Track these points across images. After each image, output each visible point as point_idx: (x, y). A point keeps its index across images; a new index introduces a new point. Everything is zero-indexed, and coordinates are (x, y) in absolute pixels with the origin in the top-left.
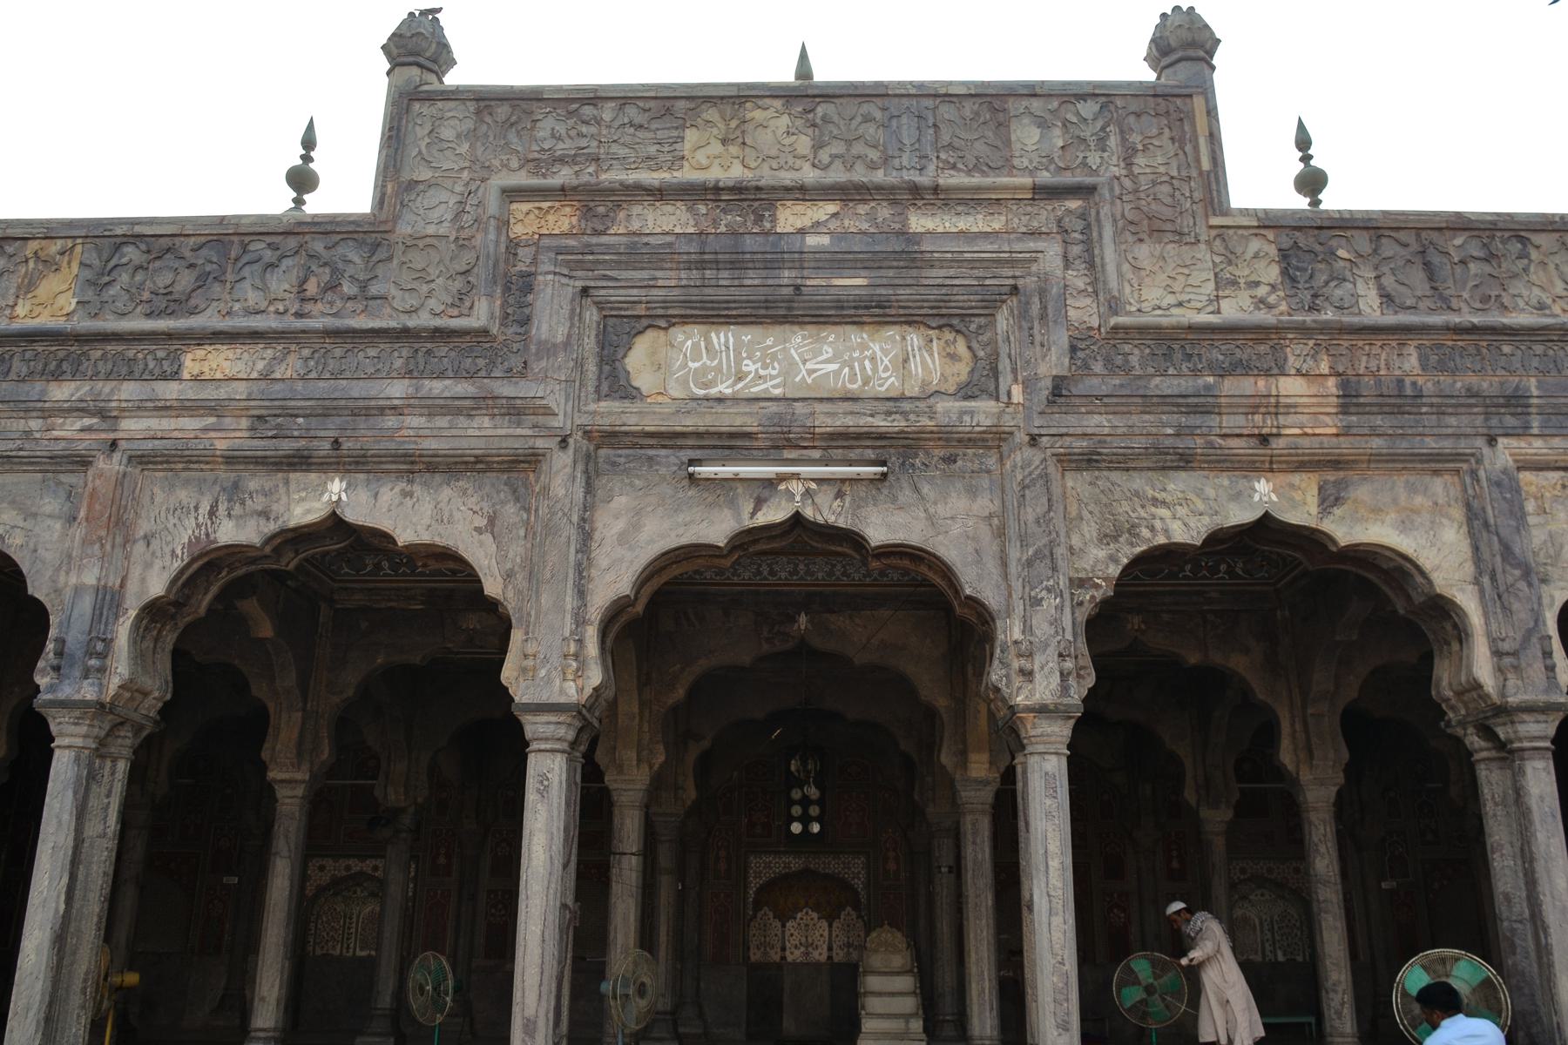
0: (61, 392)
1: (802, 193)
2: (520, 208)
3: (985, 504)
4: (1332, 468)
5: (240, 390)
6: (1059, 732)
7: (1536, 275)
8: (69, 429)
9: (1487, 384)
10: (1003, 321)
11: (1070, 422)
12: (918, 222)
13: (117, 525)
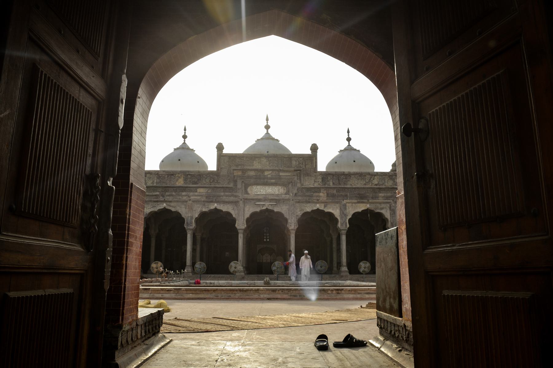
0: (184, 194)
3: (287, 207)
6: (294, 232)
7: (351, 181)
8: (185, 198)
12: (281, 174)
13: (191, 209)
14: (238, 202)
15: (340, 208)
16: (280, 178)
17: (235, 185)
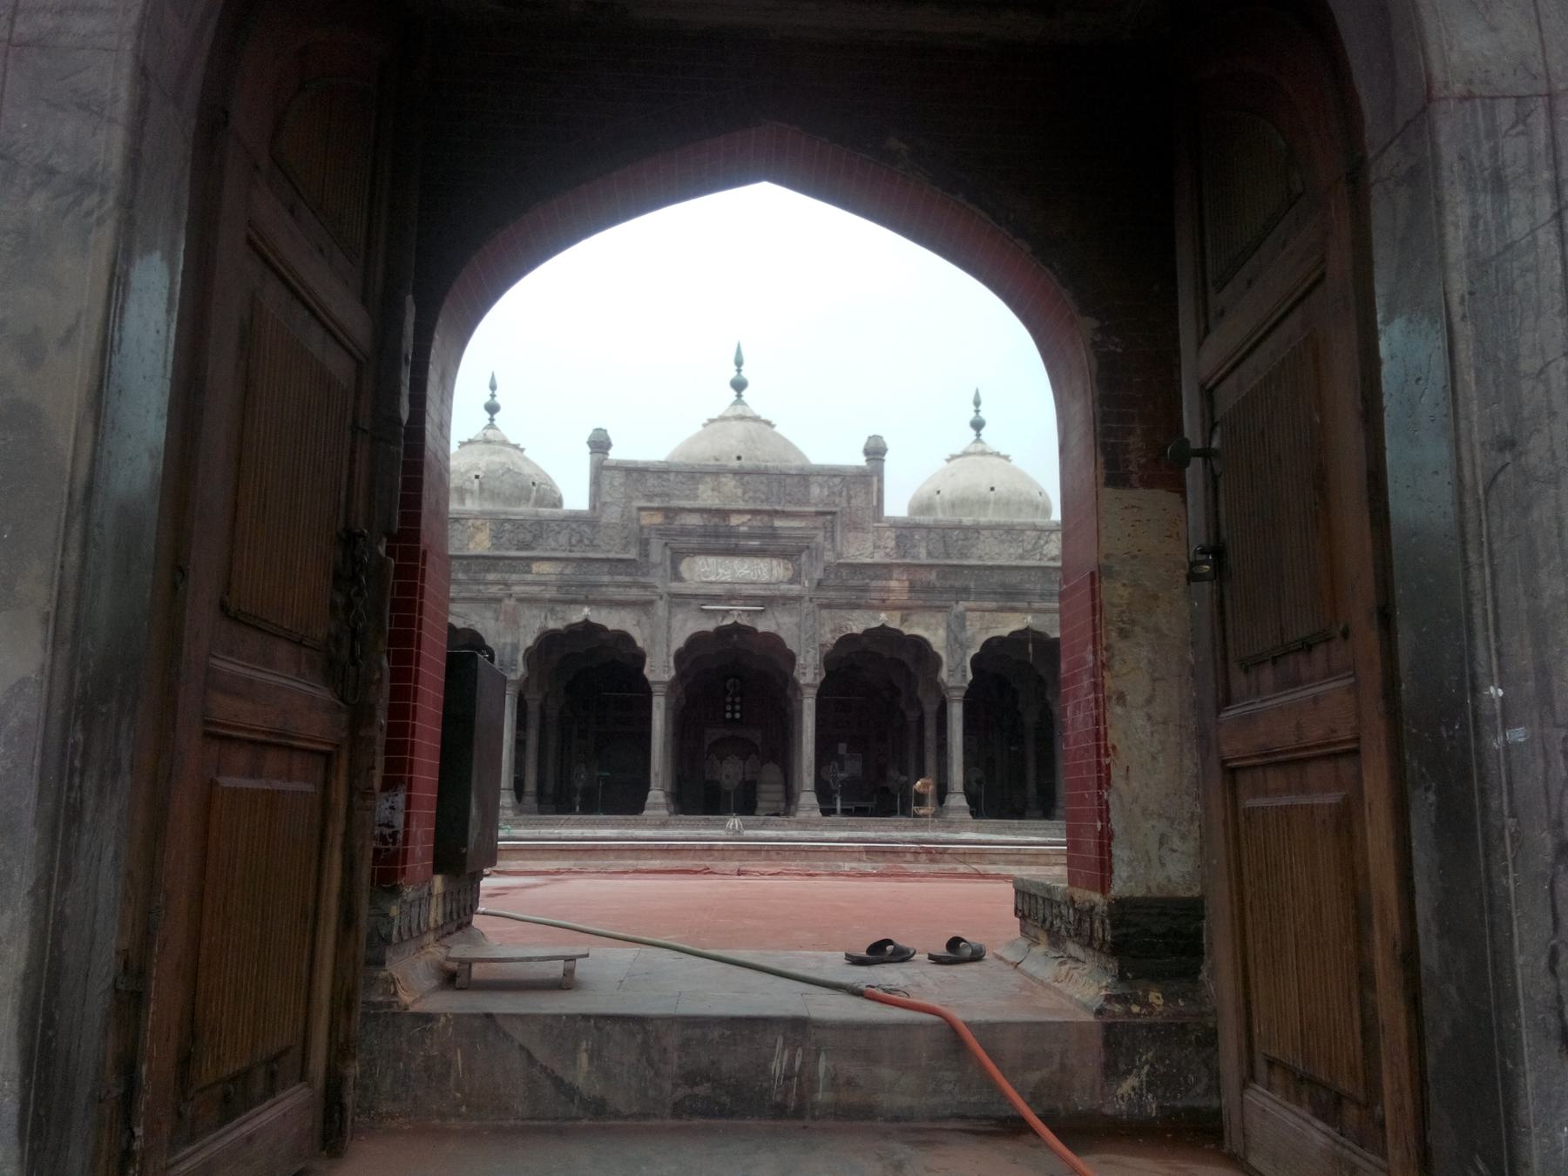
0: (491, 577)
1: (739, 512)
2: (643, 513)
3: (795, 619)
4: (906, 610)
5: (553, 578)
7: (981, 546)
8: (494, 590)
9: (957, 584)
10: (804, 557)
11: (822, 594)
12: (778, 523)
13: (513, 621)
14: (651, 603)
15: (949, 626)
16: (773, 534)
17: (645, 554)
